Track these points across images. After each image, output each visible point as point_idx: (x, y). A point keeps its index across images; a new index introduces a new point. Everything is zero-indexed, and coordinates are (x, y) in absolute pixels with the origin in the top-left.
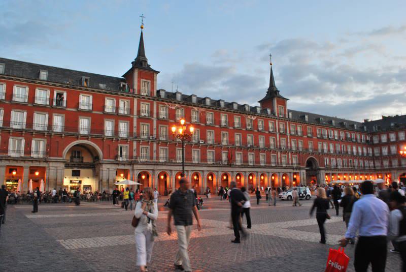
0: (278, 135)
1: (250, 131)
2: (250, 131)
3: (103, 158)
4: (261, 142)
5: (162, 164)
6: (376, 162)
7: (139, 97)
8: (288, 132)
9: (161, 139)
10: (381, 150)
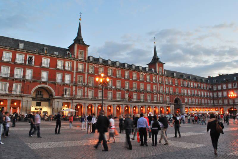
1: (142, 82)
3: (55, 95)
4: (148, 88)
5: (90, 100)
6: (215, 101)
7: (77, 60)
9: (90, 85)
10: (218, 94)
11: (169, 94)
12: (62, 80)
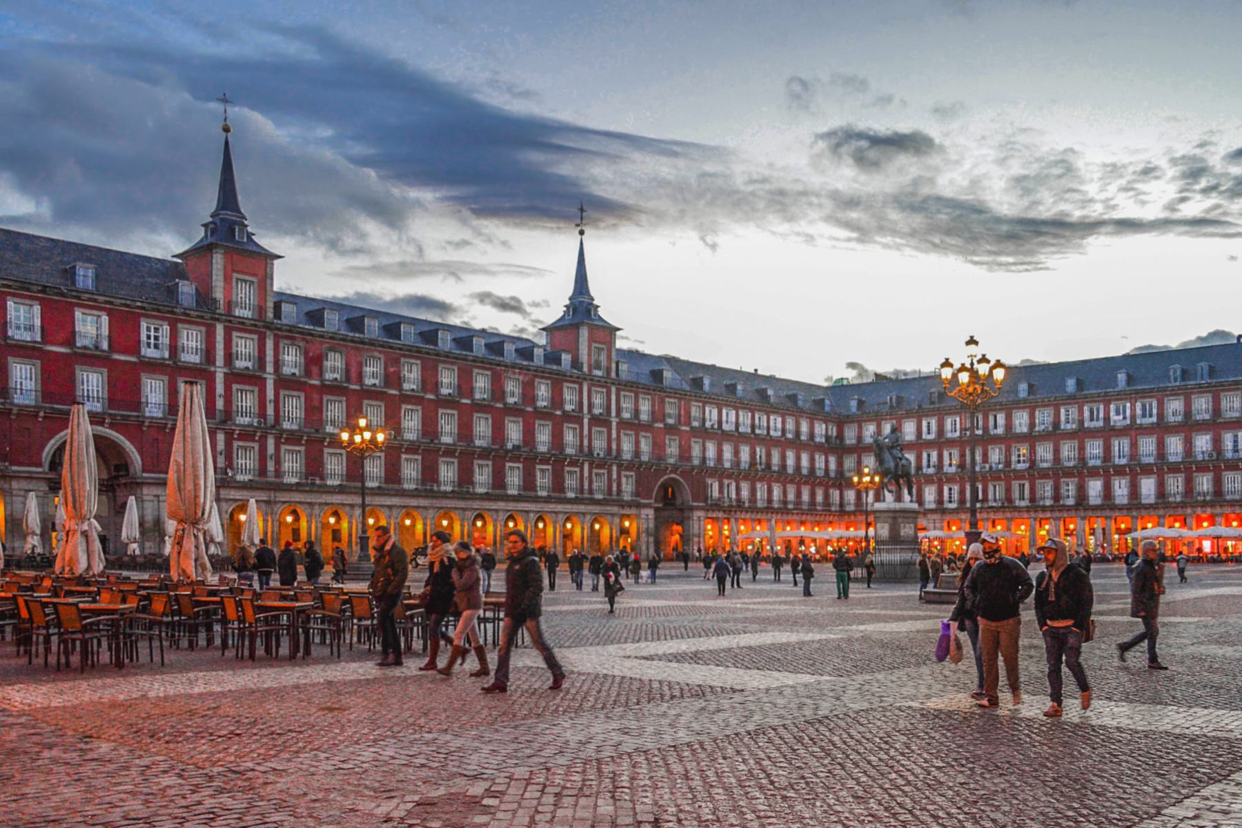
0: (586, 421)
2: (514, 411)
3: (144, 471)
4: (543, 437)
5: (290, 488)
7: (230, 321)
8: (614, 414)
11: (635, 465)
12: (39, 394)
